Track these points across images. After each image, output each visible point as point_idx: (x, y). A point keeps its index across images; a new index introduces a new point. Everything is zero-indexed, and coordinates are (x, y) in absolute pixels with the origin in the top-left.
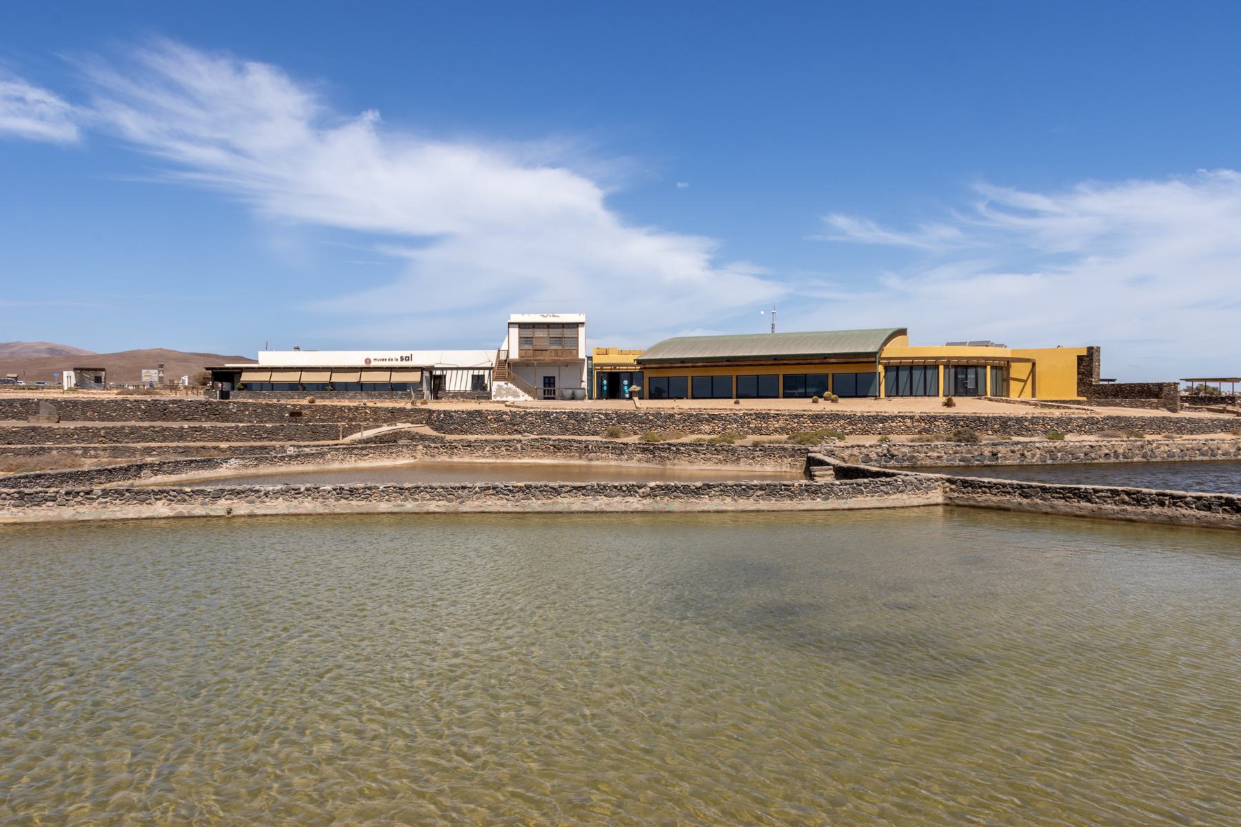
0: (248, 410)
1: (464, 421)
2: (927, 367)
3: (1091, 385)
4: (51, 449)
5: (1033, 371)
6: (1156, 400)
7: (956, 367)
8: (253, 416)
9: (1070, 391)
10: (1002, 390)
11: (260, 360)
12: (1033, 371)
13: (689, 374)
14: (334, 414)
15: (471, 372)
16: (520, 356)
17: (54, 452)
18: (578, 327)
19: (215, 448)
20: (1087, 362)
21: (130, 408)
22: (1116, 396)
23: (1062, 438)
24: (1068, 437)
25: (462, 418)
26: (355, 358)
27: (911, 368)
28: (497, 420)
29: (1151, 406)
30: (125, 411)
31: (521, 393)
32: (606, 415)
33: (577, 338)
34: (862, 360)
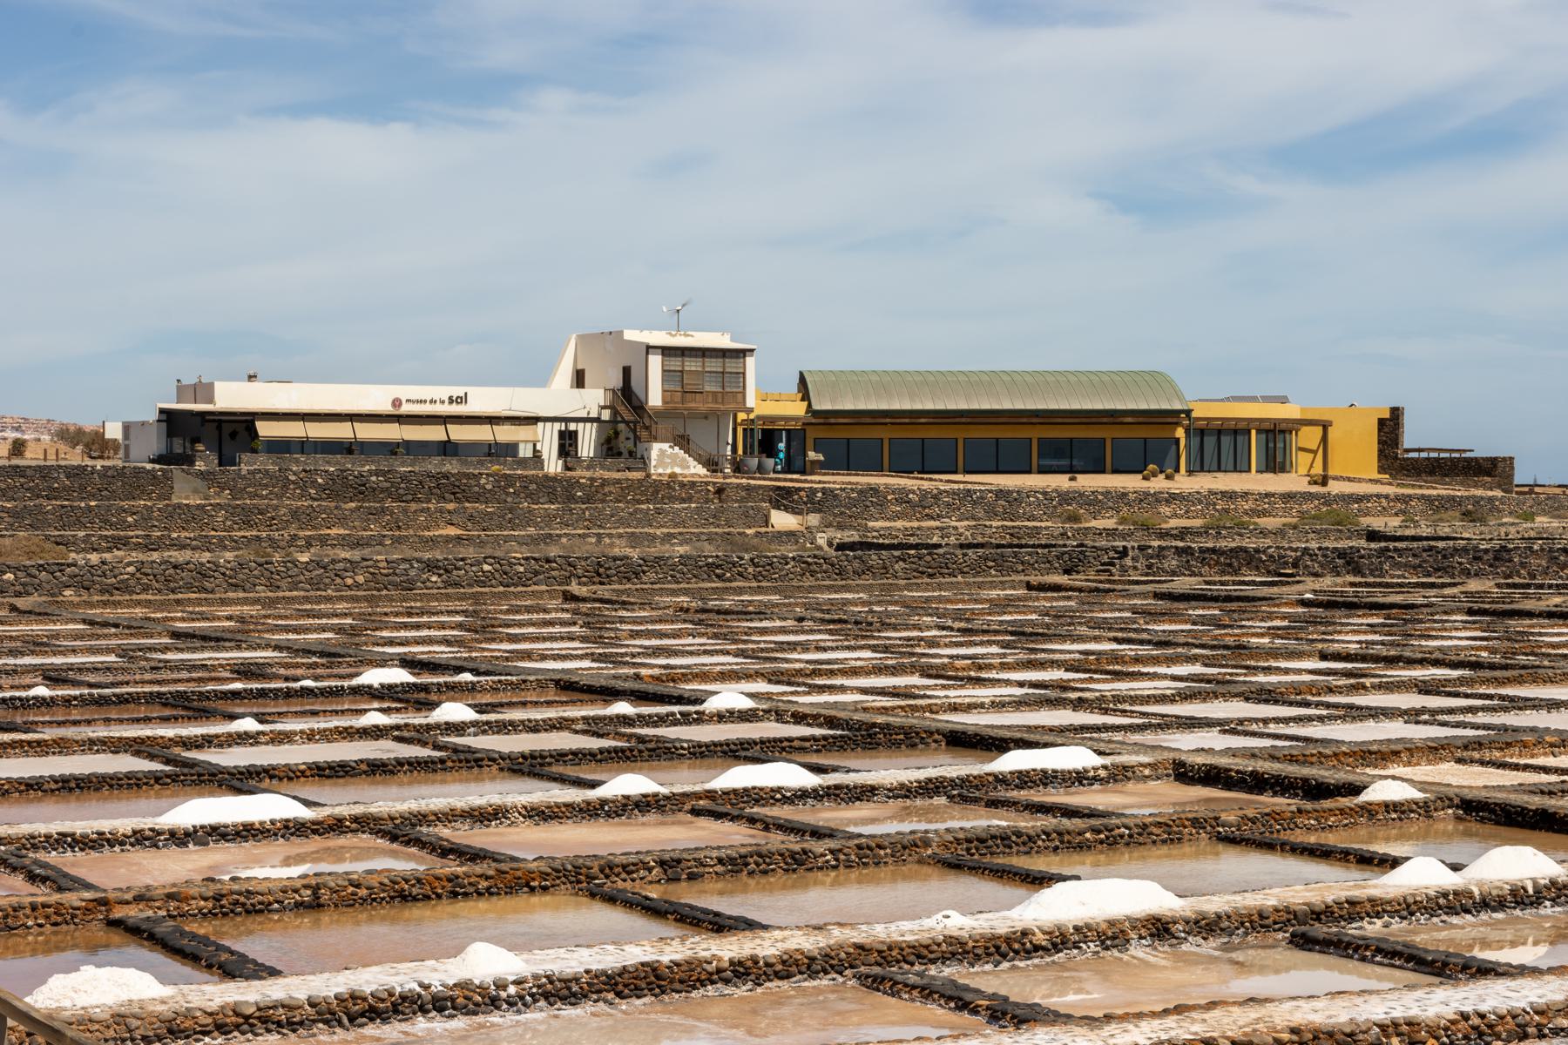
0: (512, 486)
1: (853, 504)
2: (1237, 431)
3: (1396, 458)
4: (559, 536)
5: (1324, 439)
6: (1489, 479)
7: (1267, 431)
8: (522, 495)
10: (1275, 463)
11: (217, 398)
12: (1324, 439)
13: (885, 434)
14: (657, 492)
15: (557, 426)
16: (664, 402)
17: (564, 540)
18: (745, 356)
19: (739, 534)
20: (1390, 427)
21: (293, 482)
22: (1431, 473)
23: (1533, 521)
24: (1538, 519)
25: (850, 498)
26: (376, 398)
27: (1219, 432)
28: (899, 501)
29: (1484, 486)
30: (285, 487)
31: (691, 460)
32: (1045, 493)
33: (744, 374)
34: (1170, 420)
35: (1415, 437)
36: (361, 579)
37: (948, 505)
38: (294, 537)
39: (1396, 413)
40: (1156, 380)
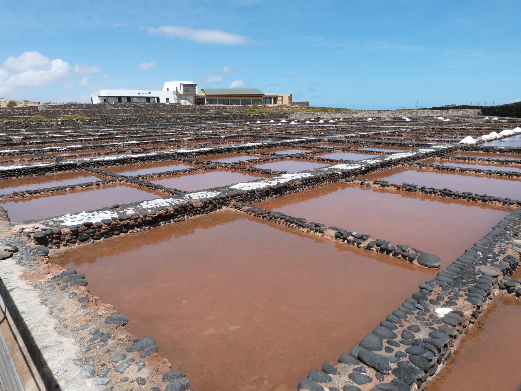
9: (287, 103)
35: (294, 100)
36: (165, 121)
37: (237, 109)
38: (136, 115)
39: (291, 95)
40: (257, 90)
